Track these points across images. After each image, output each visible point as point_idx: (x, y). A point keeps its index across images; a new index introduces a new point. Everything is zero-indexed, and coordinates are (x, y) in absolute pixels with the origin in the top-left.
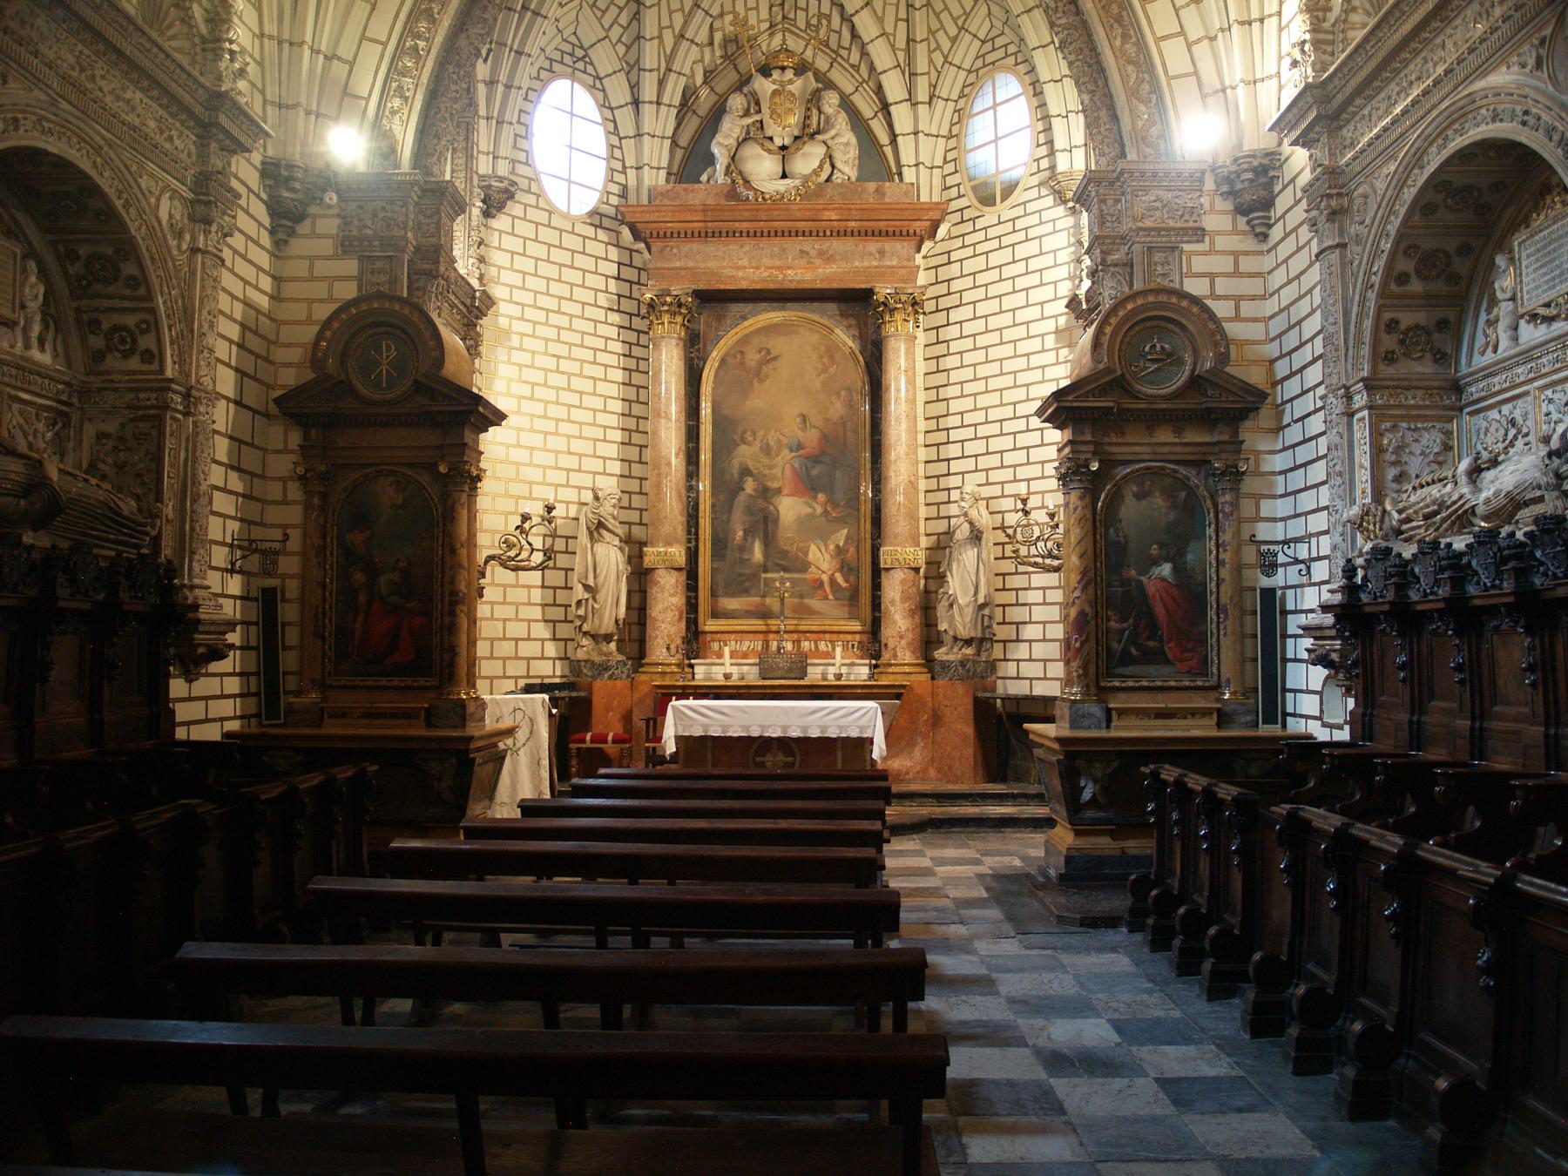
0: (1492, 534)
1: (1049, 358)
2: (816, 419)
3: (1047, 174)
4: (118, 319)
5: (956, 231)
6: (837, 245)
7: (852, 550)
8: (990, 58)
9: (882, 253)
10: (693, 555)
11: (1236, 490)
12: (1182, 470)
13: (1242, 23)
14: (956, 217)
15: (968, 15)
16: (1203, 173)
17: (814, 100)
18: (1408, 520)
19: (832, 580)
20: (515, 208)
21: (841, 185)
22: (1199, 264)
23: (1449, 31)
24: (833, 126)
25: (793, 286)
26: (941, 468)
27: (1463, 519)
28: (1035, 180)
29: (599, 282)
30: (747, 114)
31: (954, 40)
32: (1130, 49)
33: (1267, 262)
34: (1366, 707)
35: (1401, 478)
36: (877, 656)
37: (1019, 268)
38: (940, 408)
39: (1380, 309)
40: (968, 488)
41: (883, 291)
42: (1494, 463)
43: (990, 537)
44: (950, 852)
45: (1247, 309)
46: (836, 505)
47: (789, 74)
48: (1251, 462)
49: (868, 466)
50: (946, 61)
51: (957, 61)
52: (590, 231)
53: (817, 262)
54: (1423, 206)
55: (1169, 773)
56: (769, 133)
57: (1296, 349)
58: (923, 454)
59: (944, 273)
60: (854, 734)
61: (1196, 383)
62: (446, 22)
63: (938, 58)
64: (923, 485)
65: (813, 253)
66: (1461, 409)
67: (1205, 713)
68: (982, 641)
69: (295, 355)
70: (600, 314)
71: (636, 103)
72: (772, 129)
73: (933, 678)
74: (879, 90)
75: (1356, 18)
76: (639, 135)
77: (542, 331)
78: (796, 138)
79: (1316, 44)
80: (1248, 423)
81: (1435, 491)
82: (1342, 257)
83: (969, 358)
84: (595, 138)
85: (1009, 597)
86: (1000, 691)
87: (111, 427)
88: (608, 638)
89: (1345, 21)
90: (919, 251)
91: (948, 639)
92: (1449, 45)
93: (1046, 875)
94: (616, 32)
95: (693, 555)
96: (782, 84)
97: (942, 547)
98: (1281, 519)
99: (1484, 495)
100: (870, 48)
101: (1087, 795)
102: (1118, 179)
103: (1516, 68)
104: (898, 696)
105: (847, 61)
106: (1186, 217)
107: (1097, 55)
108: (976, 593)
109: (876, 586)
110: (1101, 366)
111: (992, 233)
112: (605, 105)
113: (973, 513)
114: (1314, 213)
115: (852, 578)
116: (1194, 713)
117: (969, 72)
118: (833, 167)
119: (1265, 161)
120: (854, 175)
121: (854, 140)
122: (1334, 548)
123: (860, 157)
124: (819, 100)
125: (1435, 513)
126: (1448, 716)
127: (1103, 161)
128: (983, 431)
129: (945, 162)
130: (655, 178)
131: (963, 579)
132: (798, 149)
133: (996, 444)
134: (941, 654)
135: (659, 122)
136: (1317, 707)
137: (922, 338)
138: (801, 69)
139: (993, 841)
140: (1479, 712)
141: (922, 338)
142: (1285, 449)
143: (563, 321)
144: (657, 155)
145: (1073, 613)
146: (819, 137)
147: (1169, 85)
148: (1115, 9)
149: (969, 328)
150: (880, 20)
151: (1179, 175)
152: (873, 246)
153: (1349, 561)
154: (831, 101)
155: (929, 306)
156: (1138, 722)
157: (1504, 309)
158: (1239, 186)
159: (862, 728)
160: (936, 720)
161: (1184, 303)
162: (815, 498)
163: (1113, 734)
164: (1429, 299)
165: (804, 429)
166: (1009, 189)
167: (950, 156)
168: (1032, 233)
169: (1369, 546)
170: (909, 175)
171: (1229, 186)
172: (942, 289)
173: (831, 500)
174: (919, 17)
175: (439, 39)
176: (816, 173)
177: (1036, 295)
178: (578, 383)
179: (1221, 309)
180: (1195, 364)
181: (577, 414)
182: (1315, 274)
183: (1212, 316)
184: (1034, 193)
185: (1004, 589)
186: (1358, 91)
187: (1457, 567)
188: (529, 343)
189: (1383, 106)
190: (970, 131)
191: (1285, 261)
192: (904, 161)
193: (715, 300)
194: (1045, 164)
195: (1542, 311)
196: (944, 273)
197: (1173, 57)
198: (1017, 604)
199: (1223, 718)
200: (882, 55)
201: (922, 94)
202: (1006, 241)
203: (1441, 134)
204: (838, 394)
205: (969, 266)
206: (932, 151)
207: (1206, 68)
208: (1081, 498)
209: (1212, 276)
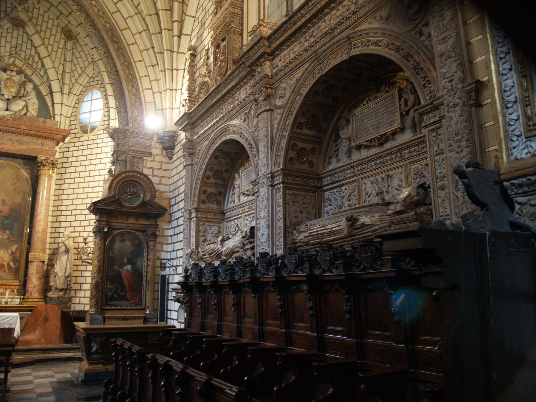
0: (225, 261)
2: (8, 202)
3: (107, 126)
5: (73, 140)
6: (25, 139)
7: (18, 253)
8: (92, 84)
9: (43, 144)
11: (155, 241)
12: (137, 233)
13: (170, 90)
14: (73, 136)
15: (86, 68)
16: (153, 135)
17: (23, 85)
18: (204, 255)
19: (9, 265)
21: (30, 117)
23: (224, 105)
24: (29, 96)
25: (5, 151)
26: (57, 225)
27: (219, 256)
28: (102, 128)
31: (80, 75)
32: (134, 91)
33: (171, 167)
34: (189, 317)
35: (204, 241)
36: (24, 295)
38: (59, 203)
39: (201, 186)
40: (66, 233)
41: (41, 158)
42: (229, 238)
43: (73, 251)
44: (42, 373)
45: (164, 181)
46: (13, 235)
47: (14, 73)
48: (161, 232)
49: (28, 222)
50: (76, 81)
51: (80, 82)
53: (16, 144)
54: (215, 156)
55: (120, 341)
56: (3, 93)
57: (177, 196)
59: (66, 155)
60: (7, 326)
61: (144, 204)
63: (73, 80)
64: (49, 230)
65: (15, 140)
66: (224, 220)
67: (139, 318)
68: (67, 290)
73: (46, 303)
74: (50, 87)
75: (201, 95)
78: (14, 97)
79: (190, 101)
80: (160, 219)
81: (212, 246)
82: (192, 168)
83: (72, 186)
85: (79, 274)
86: (72, 309)
89: (198, 96)
90: (57, 145)
91: (53, 289)
92: (224, 109)
93: (77, 380)
96: (11, 76)
98: (170, 252)
99: (225, 248)
100: (48, 71)
101: (94, 349)
102: (125, 132)
103: (240, 120)
104: (31, 311)
105: (39, 74)
106: (146, 148)
107: (123, 90)
108: (65, 272)
109: (27, 267)
110: (111, 195)
111: (85, 143)
113: (67, 243)
114: (185, 153)
115: (17, 264)
116: (135, 318)
117: (84, 87)
118: (27, 110)
119: (173, 134)
120: (35, 114)
121: (37, 102)
122: (183, 262)
123: (39, 109)
124: (25, 85)
125: (212, 253)
126: (212, 320)
127: (121, 125)
128: (74, 212)
129: (72, 116)
131: (61, 266)
132: (14, 101)
133: (78, 218)
134: (50, 294)
136: (176, 317)
138: (20, 72)
139: (62, 367)
140: (220, 319)
141: (55, 176)
142: (172, 228)
145: (94, 281)
146: (23, 98)
147: (145, 105)
148: (130, 77)
149: (73, 175)
150: (53, 62)
151: (145, 134)
152: (39, 141)
153: (186, 267)
154: (29, 87)
155: (59, 166)
156: (115, 322)
157: (237, 190)
158: (164, 141)
159: (10, 324)
160: (46, 319)
161: (142, 177)
162: (5, 232)
163: (107, 326)
164: (216, 185)
165: (3, 205)
166: (93, 129)
167: (74, 114)
168: (99, 145)
169: (193, 262)
170: (57, 118)
171: (161, 140)
172: (65, 160)
173: (12, 234)
174: (68, 65)
176: (20, 111)
177: (98, 167)
179: (154, 180)
180: (144, 197)
182: (183, 173)
183: (151, 182)
184: (101, 132)
185: (77, 271)
186: (200, 117)
187: (215, 271)
189: (206, 123)
190: (82, 107)
191: (176, 167)
192: (56, 113)
194: (106, 123)
195: (246, 192)
196: (66, 155)
197: (147, 96)
198: (81, 276)
199: (146, 320)
200: (52, 74)
201: (66, 91)
202: (90, 147)
203: (220, 135)
204: (19, 194)
205: (76, 153)
206: (67, 111)
207: (158, 101)
208: (100, 240)
209: (153, 169)
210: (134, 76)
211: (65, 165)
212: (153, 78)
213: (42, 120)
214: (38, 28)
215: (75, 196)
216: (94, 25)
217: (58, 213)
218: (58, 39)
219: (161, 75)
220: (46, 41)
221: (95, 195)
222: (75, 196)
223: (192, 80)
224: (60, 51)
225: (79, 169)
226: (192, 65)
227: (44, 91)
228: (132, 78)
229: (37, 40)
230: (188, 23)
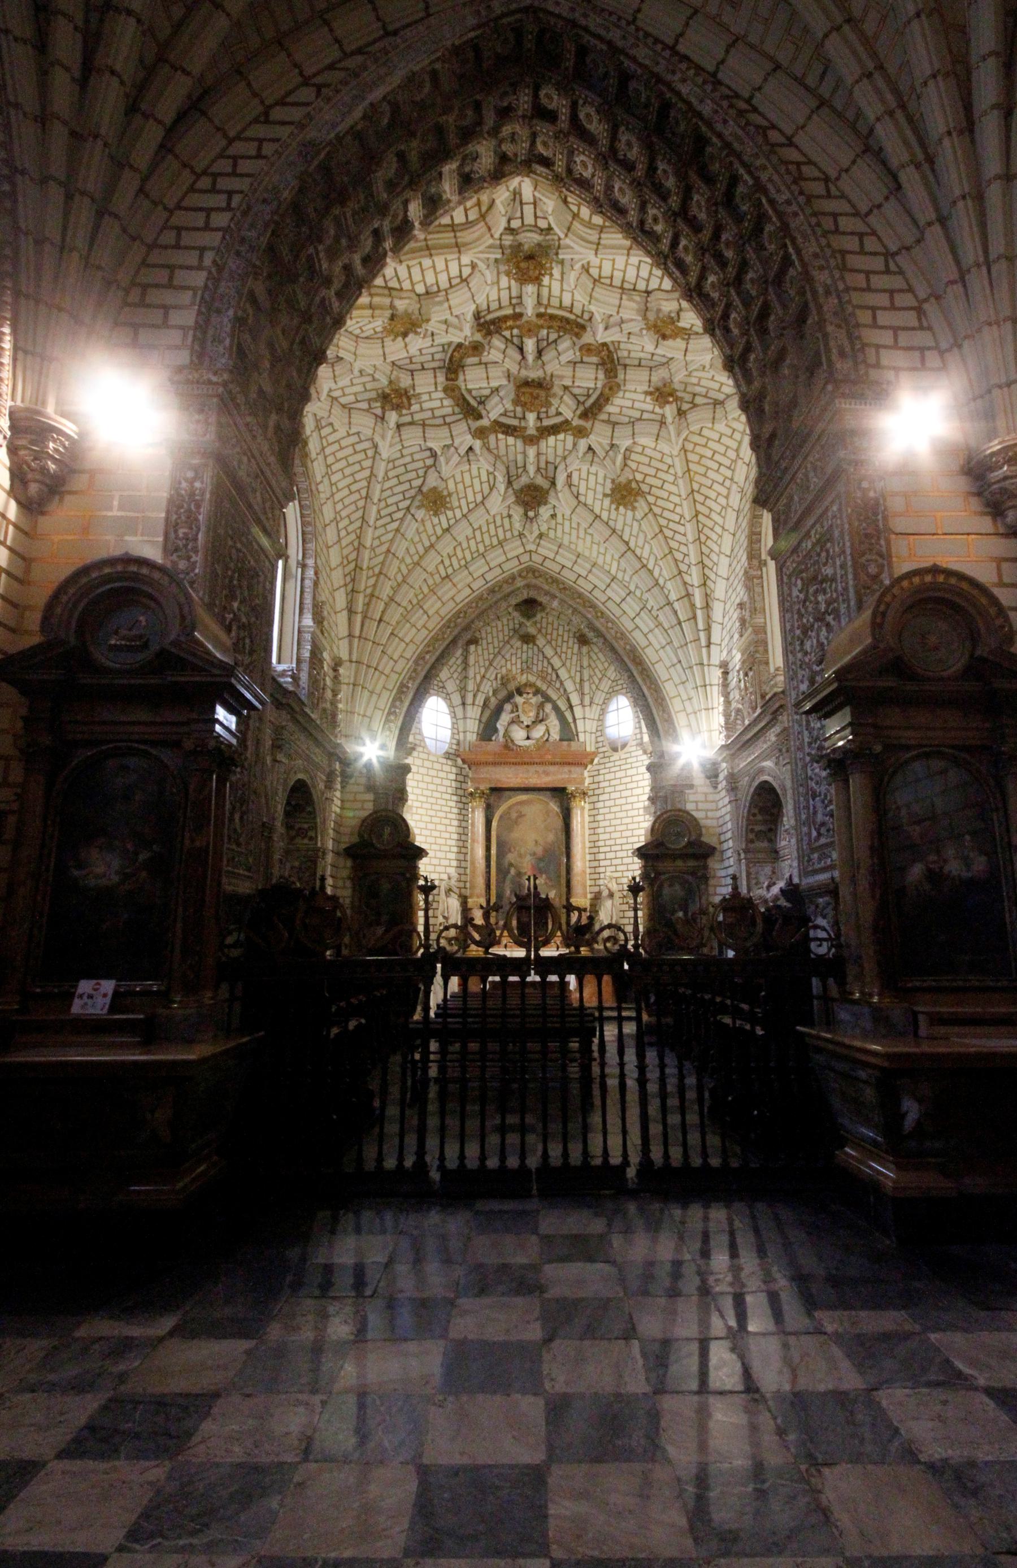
1: (641, 818)
6: (552, 769)
11: (707, 885)
17: (541, 706)
20: (415, 754)
22: (692, 798)
26: (596, 864)
29: (448, 783)
30: (512, 712)
31: (600, 680)
37: (628, 780)
38: (595, 838)
41: (571, 788)
43: (617, 895)
52: (444, 761)
58: (588, 857)
59: (596, 779)
61: (690, 844)
62: (407, 704)
63: (594, 687)
70: (448, 797)
71: (464, 704)
72: (523, 718)
74: (568, 700)
76: (465, 718)
77: (425, 805)
79: (727, 729)
83: (608, 817)
84: (446, 720)
94: (455, 675)
97: (597, 897)
112: (451, 706)
113: (610, 885)
130: (472, 737)
137: (587, 806)
138: (537, 692)
141: (587, 806)
143: (433, 801)
144: (473, 726)
149: (607, 804)
152: (566, 769)
154: (548, 707)
155: (590, 793)
164: (765, 822)
166: (624, 746)
172: (595, 786)
173: (549, 878)
175: (405, 709)
177: (636, 792)
178: (439, 827)
188: (420, 811)
193: (498, 791)
196: (596, 779)
200: (569, 686)
205: (607, 777)
211: (597, 792)
212: (684, 697)
213: (565, 743)
215: (612, 829)
216: (613, 649)
217: (596, 850)
218: (571, 644)
219: (693, 693)
220: (559, 650)
221: (636, 839)
222: (612, 829)
223: (728, 703)
224: (575, 658)
225: (613, 795)
226: (725, 685)
227: (562, 705)
228: (661, 701)
229: (549, 651)
230: (716, 629)
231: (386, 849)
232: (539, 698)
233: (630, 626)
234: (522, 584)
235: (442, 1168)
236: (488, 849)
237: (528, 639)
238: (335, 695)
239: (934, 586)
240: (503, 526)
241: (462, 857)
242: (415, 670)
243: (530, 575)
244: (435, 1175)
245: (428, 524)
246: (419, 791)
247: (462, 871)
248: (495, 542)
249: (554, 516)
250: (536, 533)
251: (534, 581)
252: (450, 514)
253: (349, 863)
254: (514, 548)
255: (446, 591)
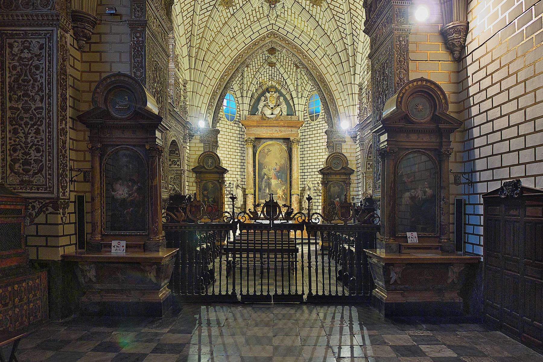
1: (324, 154)
2: (278, 164)
4: (174, 159)
5: (306, 125)
6: (283, 129)
10: (255, 191)
28: (321, 117)
41: (292, 139)
58: (300, 171)
59: (304, 134)
69: (193, 160)
74: (291, 94)
87: (173, 177)
88: (239, 208)
95: (255, 191)
135: (247, 101)
152: (290, 129)
181: (232, 163)
184: (321, 120)
188: (223, 149)
196: (304, 134)
197: (341, 109)
200: (292, 88)
201: (300, 96)
207: (347, 112)
210: (333, 99)
214: (282, 63)
219: (347, 97)
224: (294, 73)
227: (289, 98)
229: (282, 71)
231: (211, 170)
232: (277, 94)
233: (319, 63)
234: (269, 41)
235: (241, 294)
236: (254, 166)
237: (272, 65)
238: (185, 98)
239: (422, 86)
240: (259, 11)
241: (242, 170)
242: (220, 84)
243: (272, 36)
244: (239, 297)
245: (224, 12)
246: (223, 140)
247: (243, 177)
248: (256, 20)
249: (283, 7)
250: (275, 15)
251: (274, 40)
252: (234, 8)
253: (194, 175)
254: (265, 22)
255: (233, 44)
